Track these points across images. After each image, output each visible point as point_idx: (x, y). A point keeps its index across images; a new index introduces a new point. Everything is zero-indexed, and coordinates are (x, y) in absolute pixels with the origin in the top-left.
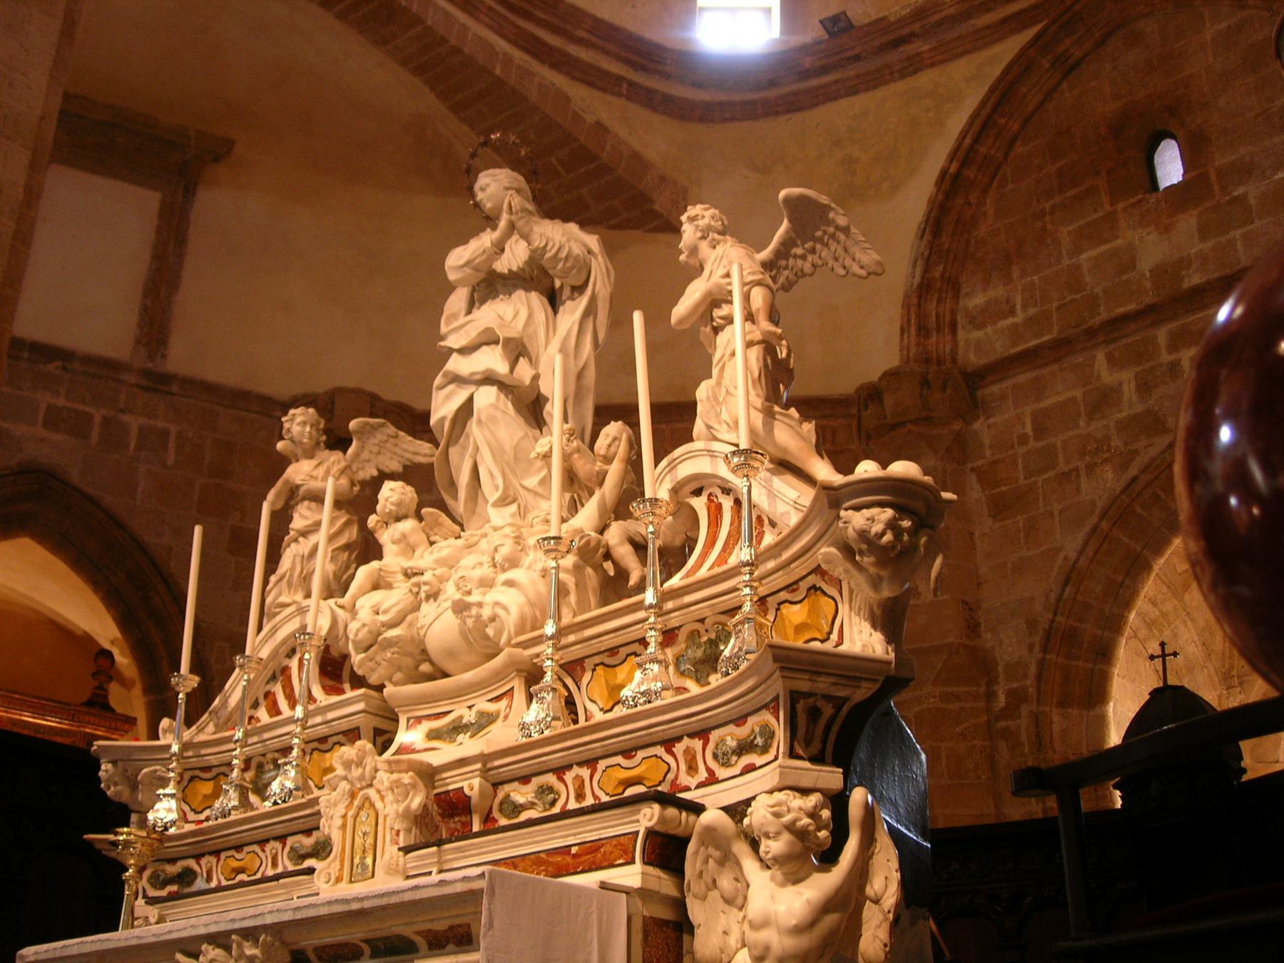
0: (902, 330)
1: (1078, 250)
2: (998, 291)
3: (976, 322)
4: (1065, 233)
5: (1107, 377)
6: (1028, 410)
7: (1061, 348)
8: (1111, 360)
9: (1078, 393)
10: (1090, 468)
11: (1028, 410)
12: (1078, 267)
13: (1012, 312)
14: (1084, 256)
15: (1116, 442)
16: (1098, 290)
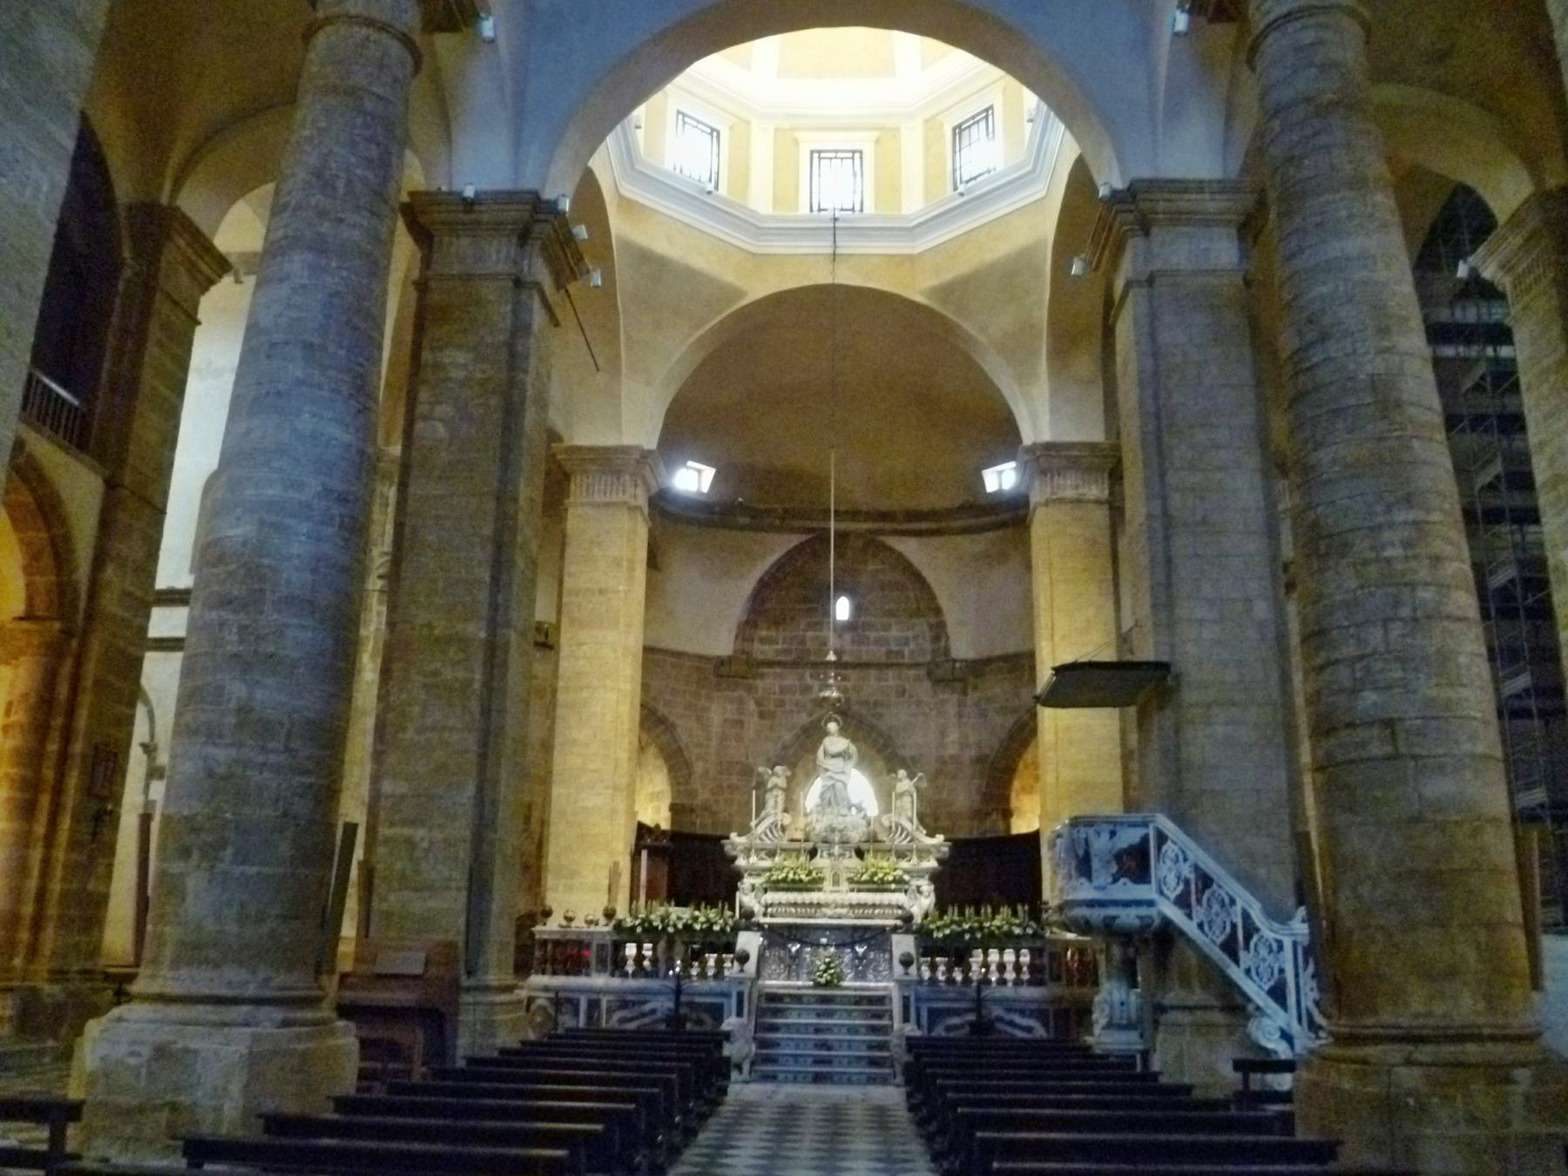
2: (773, 633)
3: (763, 641)
5: (809, 681)
7: (795, 664)
8: (811, 676)
9: (797, 683)
10: (798, 712)
12: (804, 636)
15: (809, 706)
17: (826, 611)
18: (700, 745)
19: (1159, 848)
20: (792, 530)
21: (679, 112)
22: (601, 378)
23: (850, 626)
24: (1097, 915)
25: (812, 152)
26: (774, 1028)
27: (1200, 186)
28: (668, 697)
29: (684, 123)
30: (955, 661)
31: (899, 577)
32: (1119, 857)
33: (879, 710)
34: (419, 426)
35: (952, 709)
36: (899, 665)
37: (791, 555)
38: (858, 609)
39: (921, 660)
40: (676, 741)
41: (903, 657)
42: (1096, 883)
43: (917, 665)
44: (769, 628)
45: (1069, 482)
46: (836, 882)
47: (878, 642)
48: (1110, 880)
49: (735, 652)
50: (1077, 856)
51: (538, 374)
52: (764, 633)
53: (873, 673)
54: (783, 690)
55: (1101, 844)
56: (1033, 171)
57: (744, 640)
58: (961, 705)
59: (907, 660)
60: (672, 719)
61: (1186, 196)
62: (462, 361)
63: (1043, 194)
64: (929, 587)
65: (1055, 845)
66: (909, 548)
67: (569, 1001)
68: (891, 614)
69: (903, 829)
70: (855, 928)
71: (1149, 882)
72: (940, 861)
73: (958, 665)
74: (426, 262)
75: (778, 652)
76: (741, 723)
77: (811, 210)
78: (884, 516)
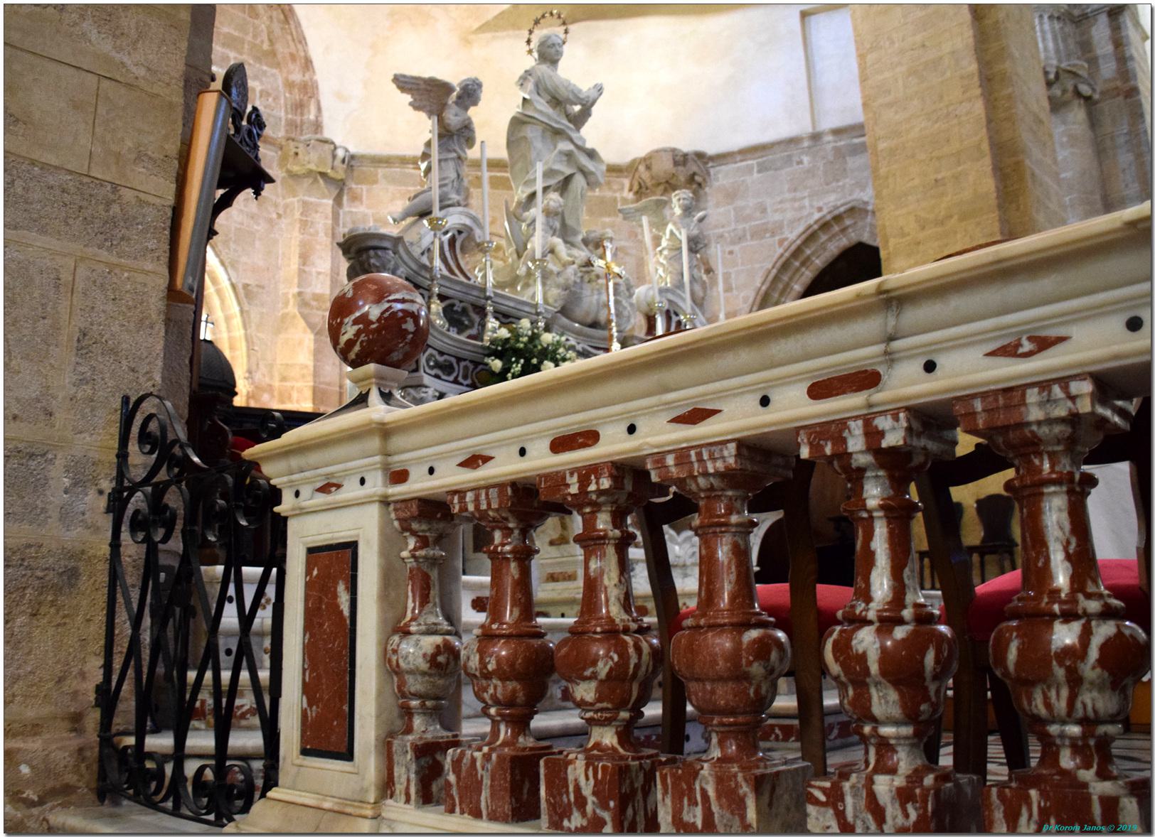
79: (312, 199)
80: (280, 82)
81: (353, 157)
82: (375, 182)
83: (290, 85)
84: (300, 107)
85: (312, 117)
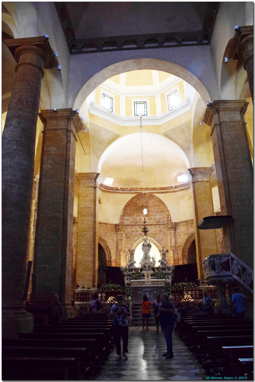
0: (120, 219)
1: (137, 217)
2: (129, 218)
3: (127, 220)
4: (136, 215)
5: (138, 229)
6: (130, 230)
8: (138, 228)
9: (135, 230)
10: (136, 237)
11: (130, 230)
12: (136, 218)
13: (130, 220)
14: (137, 218)
15: (138, 235)
16: (138, 221)
17: (142, 212)
18: (112, 246)
19: (232, 262)
20: (132, 193)
21: (103, 94)
22: (87, 156)
23: (147, 215)
24: (217, 279)
25: (134, 102)
26: (137, 312)
27: (230, 102)
28: (104, 234)
29: (104, 96)
30: (173, 223)
31: (158, 203)
32: (222, 264)
33: (155, 235)
34: (44, 166)
35: (173, 234)
36: (159, 225)
37: (132, 199)
38: (148, 211)
39: (165, 223)
40: (106, 245)
41: (160, 222)
42: (217, 271)
43: (163, 224)
44: (128, 217)
45: (200, 177)
46: (148, 277)
47: (154, 219)
48: (220, 271)
49: (120, 223)
50: (212, 265)
51: (72, 152)
52: (127, 218)
53: (153, 226)
54: (131, 231)
55: (217, 262)
56: (187, 104)
57: (122, 220)
58: (175, 233)
59: (161, 223)
60: (106, 239)
61: (227, 104)
62: (54, 150)
63: (190, 109)
64: (166, 206)
65: (205, 263)
66: (160, 196)
67: (85, 308)
68: (157, 212)
69: (163, 263)
70: (154, 287)
71: (230, 271)
72: (172, 270)
73: (173, 224)
74: (45, 127)
75: (130, 222)
76: (122, 240)
77: (135, 116)
78: (154, 189)
79: (171, 231)
80: (165, 214)
81: (176, 223)
82: (180, 226)
83: (166, 215)
84: (168, 218)
85: (170, 219)
